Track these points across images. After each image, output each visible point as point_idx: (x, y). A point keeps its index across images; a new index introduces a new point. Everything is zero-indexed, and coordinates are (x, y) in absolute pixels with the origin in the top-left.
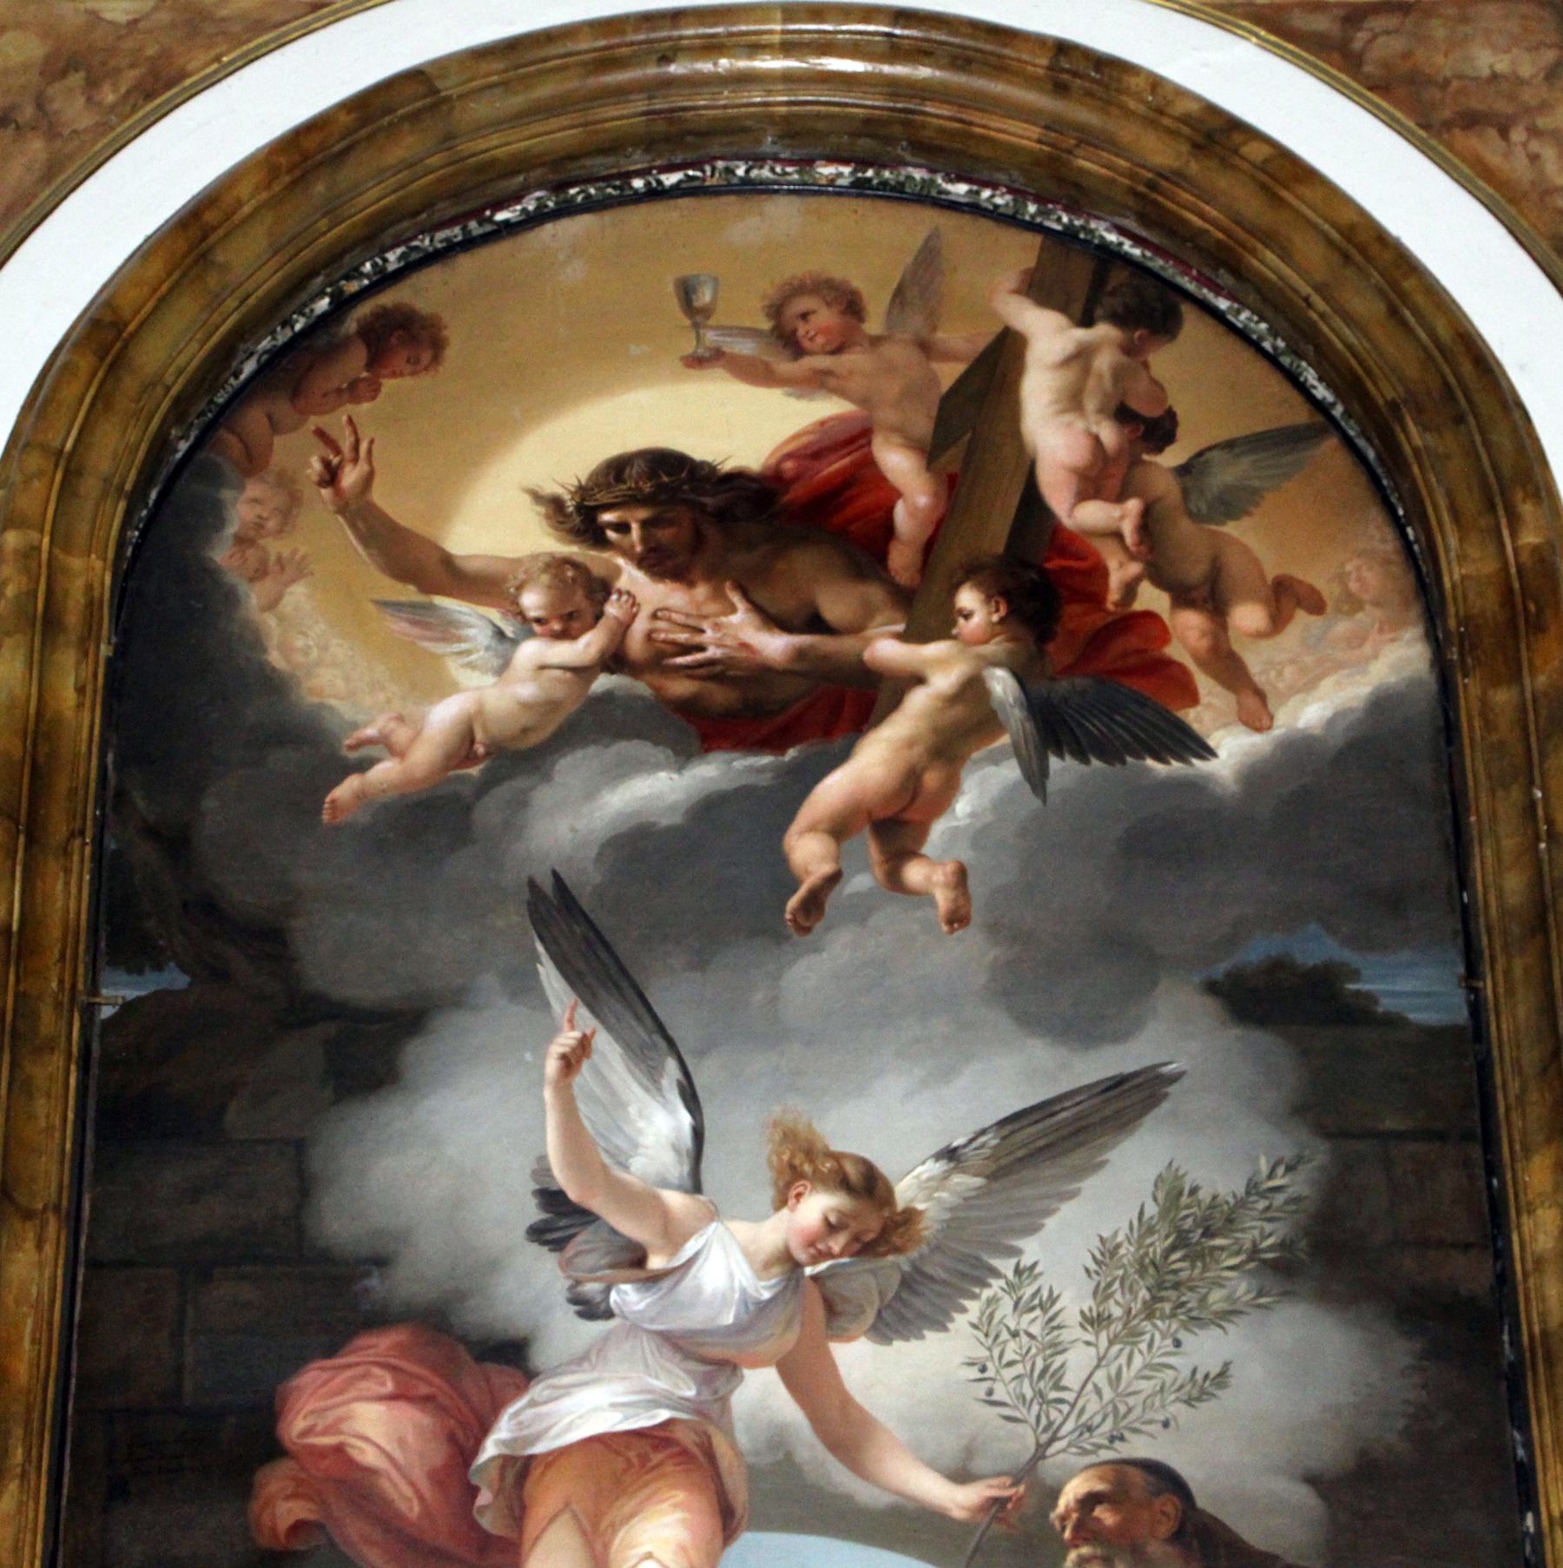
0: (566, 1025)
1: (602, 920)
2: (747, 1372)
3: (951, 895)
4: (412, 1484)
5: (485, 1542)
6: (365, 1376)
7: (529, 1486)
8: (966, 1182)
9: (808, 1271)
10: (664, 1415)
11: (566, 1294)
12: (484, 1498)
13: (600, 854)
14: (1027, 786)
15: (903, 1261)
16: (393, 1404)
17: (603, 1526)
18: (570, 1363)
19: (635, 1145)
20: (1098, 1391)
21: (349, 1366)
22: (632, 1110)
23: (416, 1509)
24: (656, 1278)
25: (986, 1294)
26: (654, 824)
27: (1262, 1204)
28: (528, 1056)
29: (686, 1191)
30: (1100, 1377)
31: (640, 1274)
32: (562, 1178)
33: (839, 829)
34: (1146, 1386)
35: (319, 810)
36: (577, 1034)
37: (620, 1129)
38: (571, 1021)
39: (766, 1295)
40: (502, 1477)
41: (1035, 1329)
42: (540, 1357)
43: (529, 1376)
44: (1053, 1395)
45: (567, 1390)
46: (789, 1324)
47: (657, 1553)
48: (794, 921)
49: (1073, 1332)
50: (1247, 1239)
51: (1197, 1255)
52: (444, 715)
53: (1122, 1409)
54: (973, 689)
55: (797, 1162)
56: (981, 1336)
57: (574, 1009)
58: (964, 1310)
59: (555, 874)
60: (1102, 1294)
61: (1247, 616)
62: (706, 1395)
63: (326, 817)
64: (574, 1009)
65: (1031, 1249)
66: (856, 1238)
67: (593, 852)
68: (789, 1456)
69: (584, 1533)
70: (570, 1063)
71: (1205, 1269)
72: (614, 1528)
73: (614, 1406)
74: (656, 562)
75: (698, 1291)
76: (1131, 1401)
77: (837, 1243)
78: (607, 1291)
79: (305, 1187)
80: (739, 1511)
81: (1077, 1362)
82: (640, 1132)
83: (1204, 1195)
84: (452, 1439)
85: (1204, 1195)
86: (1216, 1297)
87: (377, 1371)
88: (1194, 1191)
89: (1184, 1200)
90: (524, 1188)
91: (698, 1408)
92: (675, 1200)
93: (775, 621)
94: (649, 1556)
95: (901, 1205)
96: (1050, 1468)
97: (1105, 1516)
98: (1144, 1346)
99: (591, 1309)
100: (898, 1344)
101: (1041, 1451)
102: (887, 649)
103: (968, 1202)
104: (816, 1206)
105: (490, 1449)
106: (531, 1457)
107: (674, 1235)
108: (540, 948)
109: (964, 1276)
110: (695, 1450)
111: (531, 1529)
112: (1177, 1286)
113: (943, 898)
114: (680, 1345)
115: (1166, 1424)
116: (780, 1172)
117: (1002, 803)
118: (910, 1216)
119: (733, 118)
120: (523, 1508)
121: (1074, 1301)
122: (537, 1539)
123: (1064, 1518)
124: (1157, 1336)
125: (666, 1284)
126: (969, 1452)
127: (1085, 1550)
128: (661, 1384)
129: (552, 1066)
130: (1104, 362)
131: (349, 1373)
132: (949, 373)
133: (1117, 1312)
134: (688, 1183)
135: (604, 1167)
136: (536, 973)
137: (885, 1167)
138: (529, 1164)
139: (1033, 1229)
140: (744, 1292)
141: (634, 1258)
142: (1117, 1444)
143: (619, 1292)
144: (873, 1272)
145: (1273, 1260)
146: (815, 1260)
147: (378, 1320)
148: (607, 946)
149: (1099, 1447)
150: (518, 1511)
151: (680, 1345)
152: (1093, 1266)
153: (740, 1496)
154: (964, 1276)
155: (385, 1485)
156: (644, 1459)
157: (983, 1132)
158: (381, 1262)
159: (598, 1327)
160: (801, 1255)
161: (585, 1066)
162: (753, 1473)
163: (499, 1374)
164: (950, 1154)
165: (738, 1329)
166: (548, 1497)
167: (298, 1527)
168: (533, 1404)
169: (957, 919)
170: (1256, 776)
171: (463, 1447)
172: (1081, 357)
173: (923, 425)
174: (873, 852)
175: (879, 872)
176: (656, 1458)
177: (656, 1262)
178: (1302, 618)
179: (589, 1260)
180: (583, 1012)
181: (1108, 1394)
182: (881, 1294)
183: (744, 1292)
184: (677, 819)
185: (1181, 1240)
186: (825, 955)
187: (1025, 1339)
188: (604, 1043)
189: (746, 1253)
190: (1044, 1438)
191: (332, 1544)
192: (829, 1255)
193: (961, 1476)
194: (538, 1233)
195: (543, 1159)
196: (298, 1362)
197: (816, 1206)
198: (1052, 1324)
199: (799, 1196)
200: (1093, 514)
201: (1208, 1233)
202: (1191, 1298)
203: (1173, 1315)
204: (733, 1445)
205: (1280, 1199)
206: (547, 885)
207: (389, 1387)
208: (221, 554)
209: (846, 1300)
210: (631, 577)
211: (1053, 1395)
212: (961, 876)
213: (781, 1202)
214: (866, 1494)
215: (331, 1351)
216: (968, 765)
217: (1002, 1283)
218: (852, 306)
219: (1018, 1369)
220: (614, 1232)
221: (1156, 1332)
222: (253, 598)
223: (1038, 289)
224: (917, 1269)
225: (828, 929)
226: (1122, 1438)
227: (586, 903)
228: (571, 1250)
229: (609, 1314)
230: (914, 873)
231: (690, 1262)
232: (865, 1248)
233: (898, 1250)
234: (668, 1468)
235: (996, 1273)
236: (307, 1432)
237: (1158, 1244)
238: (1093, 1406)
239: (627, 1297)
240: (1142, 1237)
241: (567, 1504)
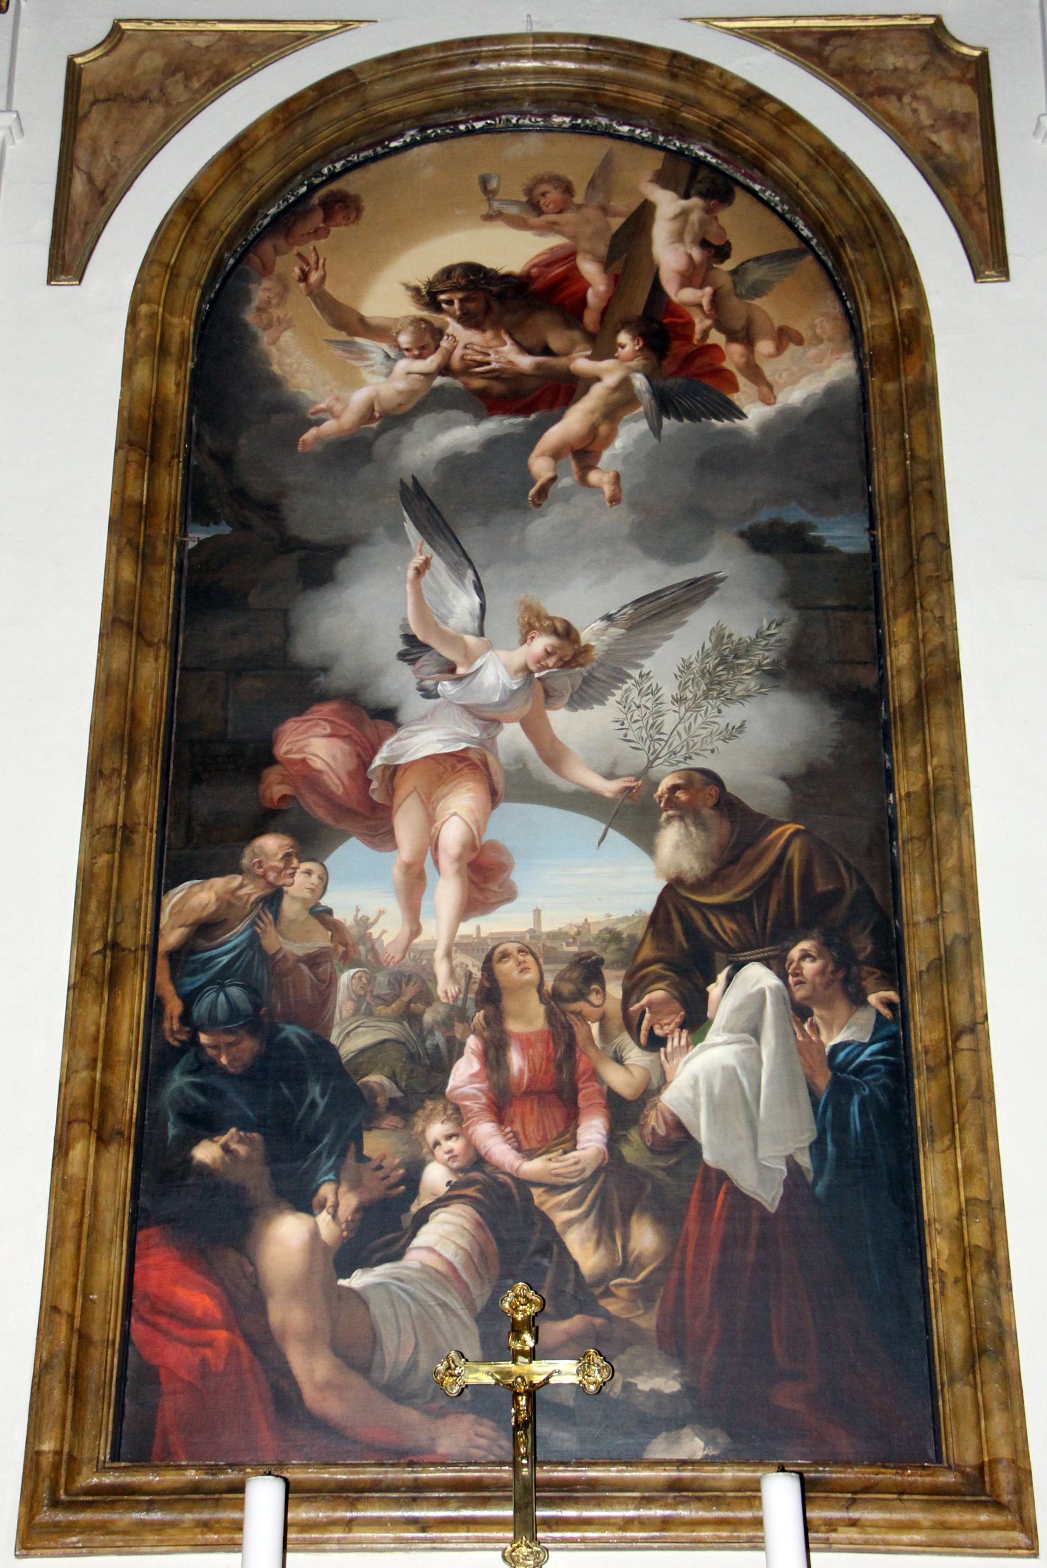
0: (418, 553)
1: (435, 499)
2: (505, 725)
3: (612, 488)
4: (339, 778)
5: (375, 807)
6: (316, 725)
7: (396, 780)
8: (616, 631)
9: (537, 675)
10: (463, 745)
11: (416, 686)
12: (374, 785)
13: (436, 467)
14: (651, 433)
15: (583, 671)
16: (330, 739)
17: (433, 799)
18: (417, 720)
19: (451, 612)
20: (679, 734)
21: (309, 720)
22: (450, 595)
23: (341, 790)
24: (461, 678)
25: (625, 687)
26: (462, 452)
27: (764, 643)
28: (399, 568)
29: (476, 636)
30: (680, 728)
31: (452, 676)
32: (415, 629)
33: (556, 455)
34: (704, 732)
35: (296, 445)
36: (423, 557)
37: (444, 605)
38: (420, 551)
39: (515, 687)
40: (383, 775)
41: (649, 704)
42: (403, 716)
43: (398, 726)
44: (657, 737)
45: (415, 733)
46: (526, 701)
47: (459, 813)
48: (533, 501)
49: (668, 706)
50: (756, 660)
51: (731, 668)
52: (359, 398)
53: (691, 744)
54: (625, 383)
55: (532, 621)
56: (621, 707)
57: (422, 545)
58: (613, 695)
59: (414, 477)
60: (683, 687)
61: (764, 347)
62: (485, 736)
63: (300, 449)
64: (422, 545)
65: (648, 665)
66: (560, 659)
67: (433, 467)
68: (525, 765)
69: (423, 803)
70: (419, 572)
71: (734, 675)
72: (438, 800)
73: (439, 741)
74: (467, 320)
75: (481, 684)
76: (696, 740)
77: (551, 662)
78: (436, 684)
79: (288, 632)
80: (500, 793)
81: (669, 720)
82: (454, 606)
83: (735, 638)
84: (359, 756)
85: (735, 638)
86: (739, 688)
87: (323, 723)
88: (730, 636)
89: (725, 640)
90: (396, 634)
91: (481, 743)
92: (471, 640)
93: (526, 350)
94: (455, 814)
95: (583, 643)
96: (654, 772)
97: (682, 796)
98: (703, 713)
99: (428, 694)
100: (580, 711)
101: (650, 764)
102: (582, 364)
103: (617, 641)
104: (541, 643)
105: (378, 761)
106: (398, 766)
107: (470, 657)
108: (405, 514)
109: (613, 678)
110: (478, 762)
111: (397, 799)
112: (720, 683)
113: (608, 490)
114: (472, 711)
115: (713, 751)
116: (523, 626)
117: (638, 442)
118: (588, 648)
119: (507, 93)
120: (393, 790)
121: (669, 690)
122: (399, 806)
123: (660, 797)
124: (710, 708)
125: (465, 681)
126: (615, 764)
127: (671, 812)
128: (462, 730)
129: (411, 573)
130: (695, 217)
131: (308, 724)
132: (616, 223)
133: (690, 696)
134: (477, 632)
135: (436, 624)
136: (403, 527)
137: (576, 624)
138: (400, 622)
139: (649, 655)
140: (504, 685)
141: (450, 669)
142: (688, 761)
143: (443, 685)
144: (569, 676)
145: (306, 430)
146: (540, 670)
147: (323, 698)
148: (439, 513)
149: (679, 762)
150: (391, 791)
151: (472, 711)
152: (678, 673)
153: (500, 784)
154: (613, 678)
155: (326, 777)
156: (453, 767)
157: (625, 607)
158: (325, 670)
159: (432, 702)
160: (533, 668)
161: (427, 573)
162: (507, 775)
163: (383, 725)
164: (609, 617)
165: (502, 704)
166: (406, 785)
167: (284, 798)
168: (399, 740)
169: (614, 500)
170: (766, 428)
171: (364, 761)
172: (683, 215)
173: (602, 250)
174: (573, 465)
175: (576, 477)
176: (460, 766)
177: (461, 671)
178: (792, 348)
179: (427, 670)
180: (426, 546)
181: (684, 736)
182: (573, 686)
183: (504, 685)
184: (474, 450)
185: (723, 661)
186: (548, 518)
187: (644, 709)
188: (437, 562)
189: (506, 666)
190: (652, 758)
191: (300, 807)
192: (547, 667)
193: (610, 776)
194: (402, 656)
195: (405, 619)
196: (283, 719)
197: (541, 643)
198: (658, 702)
199: (532, 638)
200: (687, 295)
201: (737, 657)
202: (727, 689)
203: (718, 698)
204: (498, 760)
205: (773, 640)
206: (409, 482)
207: (328, 730)
208: (250, 316)
209: (555, 689)
210: (454, 328)
211: (657, 737)
212: (617, 478)
213: (524, 641)
214: (562, 785)
215: (300, 712)
216: (622, 422)
217: (633, 681)
218: (568, 189)
219: (640, 724)
220: (440, 655)
221: (710, 706)
222: (265, 338)
223: (662, 179)
224: (590, 674)
225: (550, 505)
226: (690, 758)
227: (428, 492)
228: (419, 664)
229: (437, 696)
230: (593, 477)
231: (478, 670)
232: (565, 664)
233: (581, 665)
234: (465, 771)
235: (630, 677)
236: (287, 753)
237: (711, 663)
238: (676, 742)
239: (446, 687)
240: (703, 659)
241: (415, 789)
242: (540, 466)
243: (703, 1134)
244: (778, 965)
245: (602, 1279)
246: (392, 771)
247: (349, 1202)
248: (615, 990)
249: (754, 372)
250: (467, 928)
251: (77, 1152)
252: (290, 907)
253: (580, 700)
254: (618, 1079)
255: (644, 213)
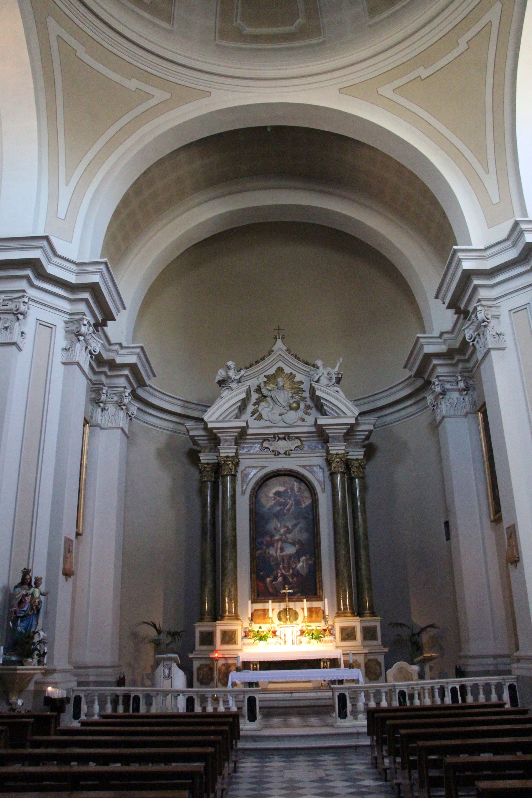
52: (269, 504)
74: (278, 496)
99: (276, 533)
104: (286, 528)
197: (286, 528)
200: (298, 493)
210: (277, 497)
242: (285, 511)
243: (300, 570)
244: (305, 556)
245: (292, 582)
246: (274, 540)
247: (273, 577)
248: (292, 559)
249: (303, 501)
250: (281, 554)
251: (253, 575)
252: (267, 553)
253: (289, 533)
254: (293, 566)
255: (294, 484)
